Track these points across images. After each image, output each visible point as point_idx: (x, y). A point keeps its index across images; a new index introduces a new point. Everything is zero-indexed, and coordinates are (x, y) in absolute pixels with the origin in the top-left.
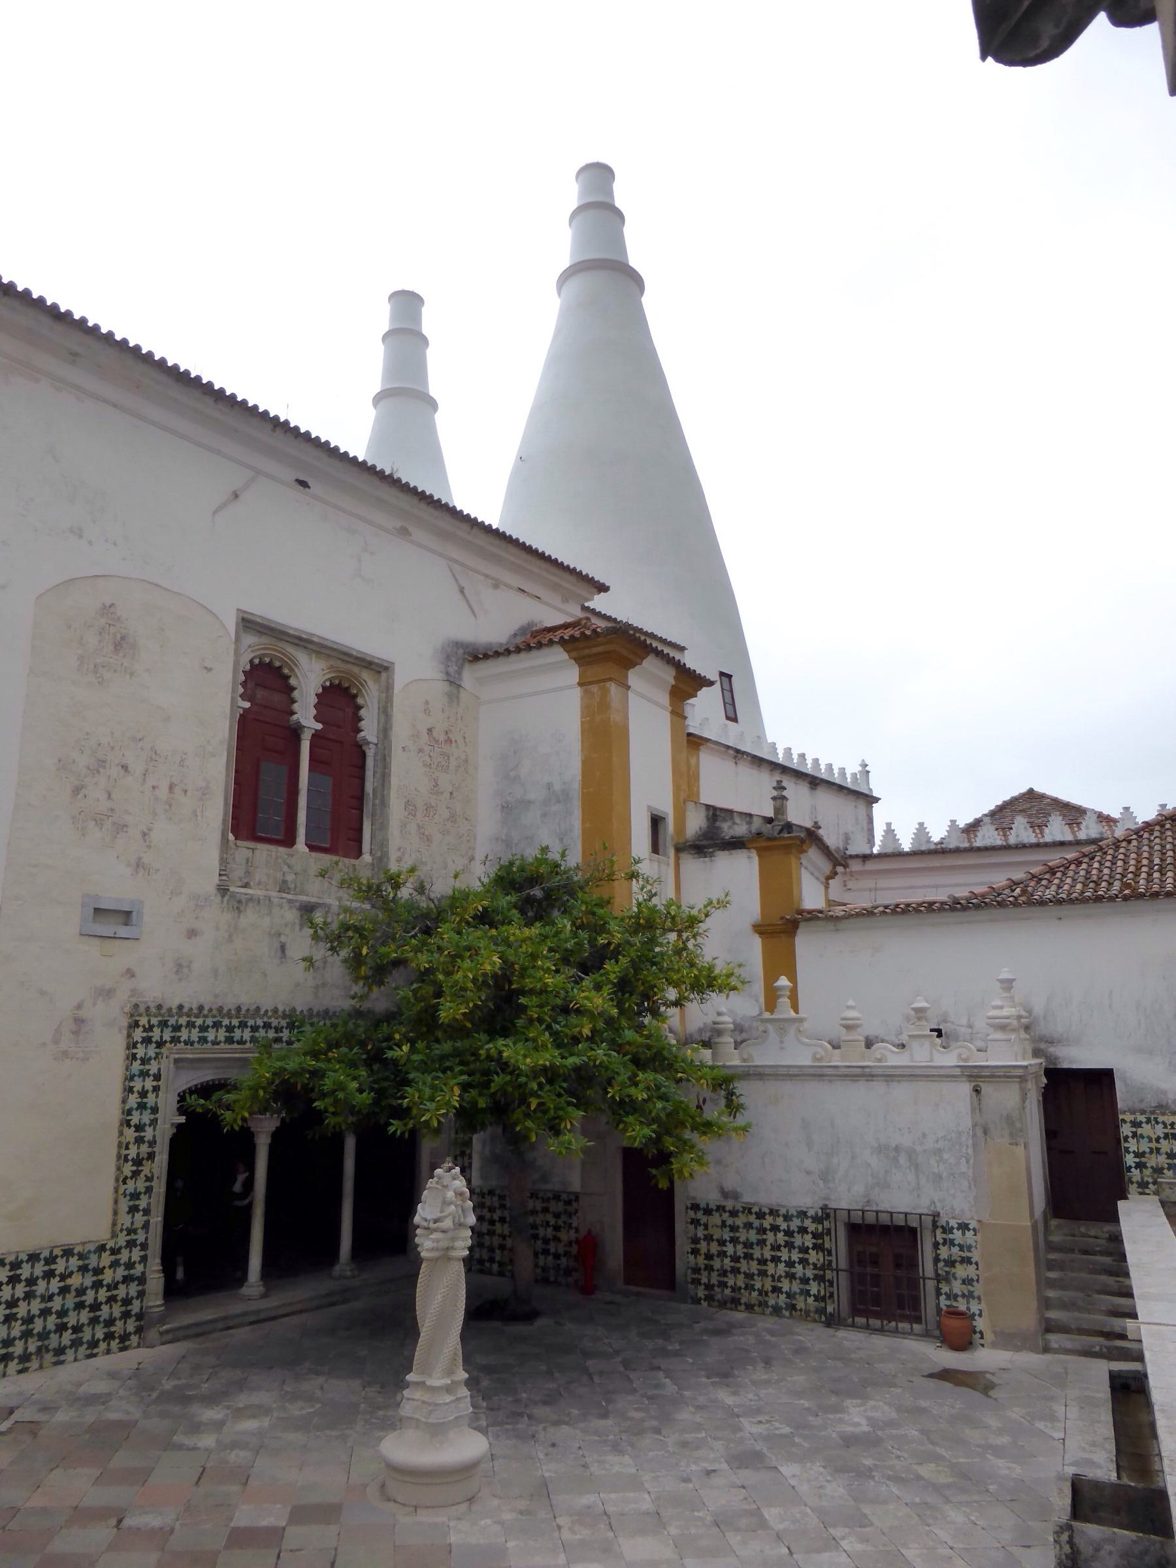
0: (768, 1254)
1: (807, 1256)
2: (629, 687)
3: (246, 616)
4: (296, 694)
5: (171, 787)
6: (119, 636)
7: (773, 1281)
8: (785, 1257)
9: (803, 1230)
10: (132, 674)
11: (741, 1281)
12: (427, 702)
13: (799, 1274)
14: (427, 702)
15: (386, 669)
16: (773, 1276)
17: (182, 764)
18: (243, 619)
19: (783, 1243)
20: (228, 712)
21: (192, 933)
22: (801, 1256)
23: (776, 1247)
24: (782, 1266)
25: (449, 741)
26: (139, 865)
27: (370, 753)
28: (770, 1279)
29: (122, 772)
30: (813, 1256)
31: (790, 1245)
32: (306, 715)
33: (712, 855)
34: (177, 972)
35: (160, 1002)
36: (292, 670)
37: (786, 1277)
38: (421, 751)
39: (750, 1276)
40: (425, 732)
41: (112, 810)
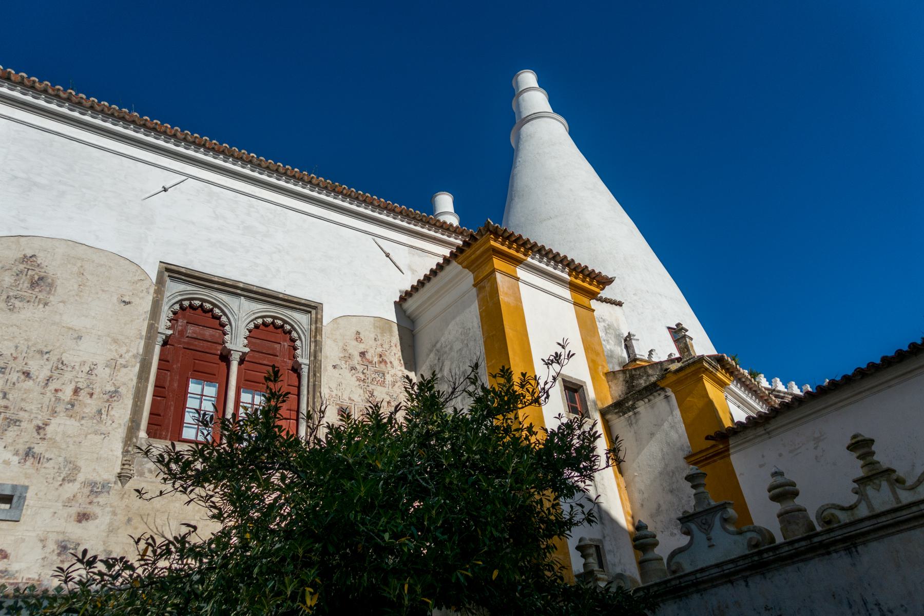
2: (518, 279)
3: (169, 267)
4: (227, 328)
5: (76, 391)
6: (36, 277)
10: (46, 304)
12: (358, 333)
14: (358, 333)
15: (315, 308)
17: (90, 372)
18: (167, 270)
20: (144, 333)
21: (83, 517)
25: (383, 361)
26: (29, 453)
27: (305, 370)
29: (23, 377)
32: (237, 343)
33: (633, 407)
34: (59, 554)
35: (36, 583)
36: (222, 311)
38: (353, 368)
41: (6, 407)
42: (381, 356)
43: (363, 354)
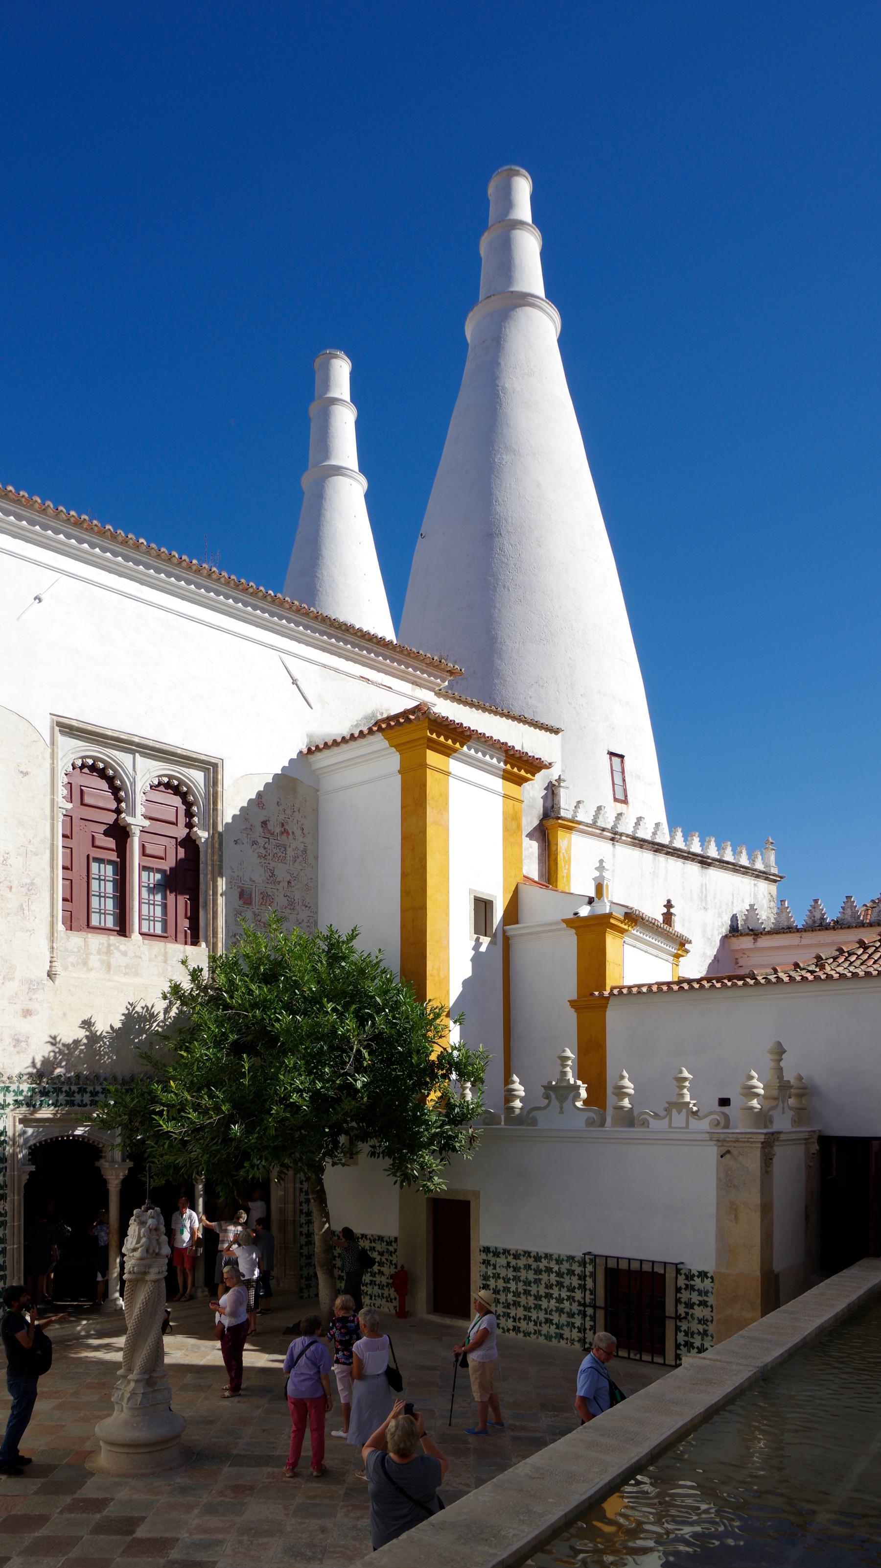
0: (542, 1292)
1: (573, 1294)
7: (546, 1314)
8: (556, 1295)
9: (571, 1272)
11: (520, 1312)
13: (567, 1310)
16: (546, 1310)
19: (555, 1283)
22: (569, 1294)
23: (549, 1286)
24: (553, 1302)
25: (285, 832)
28: (543, 1312)
30: (578, 1295)
31: (560, 1285)
37: (556, 1311)
38: (254, 843)
39: (527, 1309)
40: (258, 825)
42: (283, 825)
43: (264, 824)
